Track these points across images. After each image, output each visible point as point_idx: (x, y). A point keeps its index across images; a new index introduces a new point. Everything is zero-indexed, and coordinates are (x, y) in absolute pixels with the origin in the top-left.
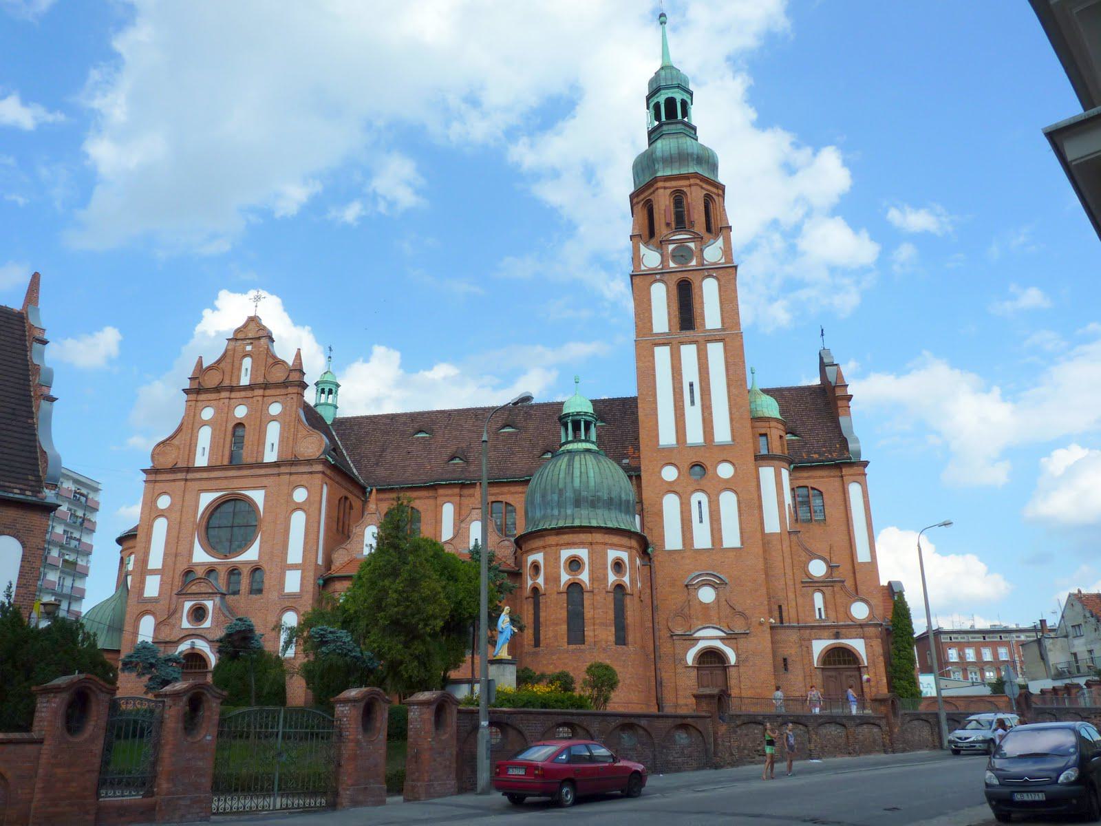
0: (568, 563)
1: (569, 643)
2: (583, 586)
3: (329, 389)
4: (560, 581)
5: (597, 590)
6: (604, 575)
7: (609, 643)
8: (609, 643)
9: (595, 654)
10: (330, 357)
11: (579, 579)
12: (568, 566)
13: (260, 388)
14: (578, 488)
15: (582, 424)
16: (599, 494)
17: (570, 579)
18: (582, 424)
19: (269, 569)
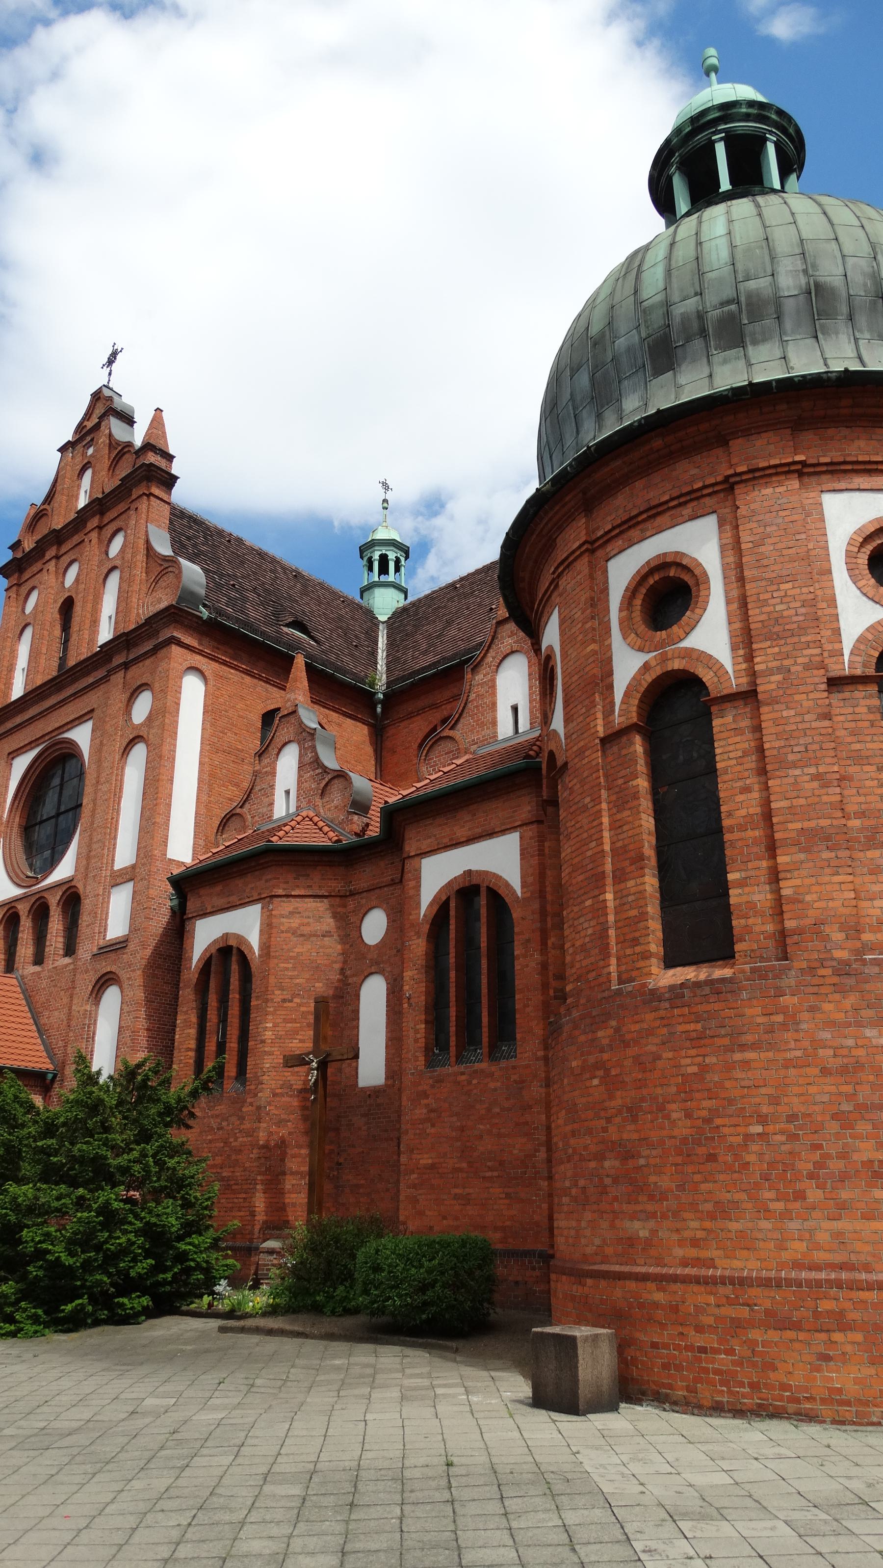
0: (638, 602)
1: (670, 962)
2: (707, 677)
3: (381, 556)
4: (610, 687)
5: (778, 678)
6: (812, 603)
7: (867, 937)
8: (867, 937)
9: (787, 1000)
10: (385, 501)
11: (689, 653)
12: (637, 615)
13: (93, 516)
14: (659, 298)
15: (720, 150)
16: (752, 285)
17: (646, 667)
18: (720, 150)
19: (88, 891)
